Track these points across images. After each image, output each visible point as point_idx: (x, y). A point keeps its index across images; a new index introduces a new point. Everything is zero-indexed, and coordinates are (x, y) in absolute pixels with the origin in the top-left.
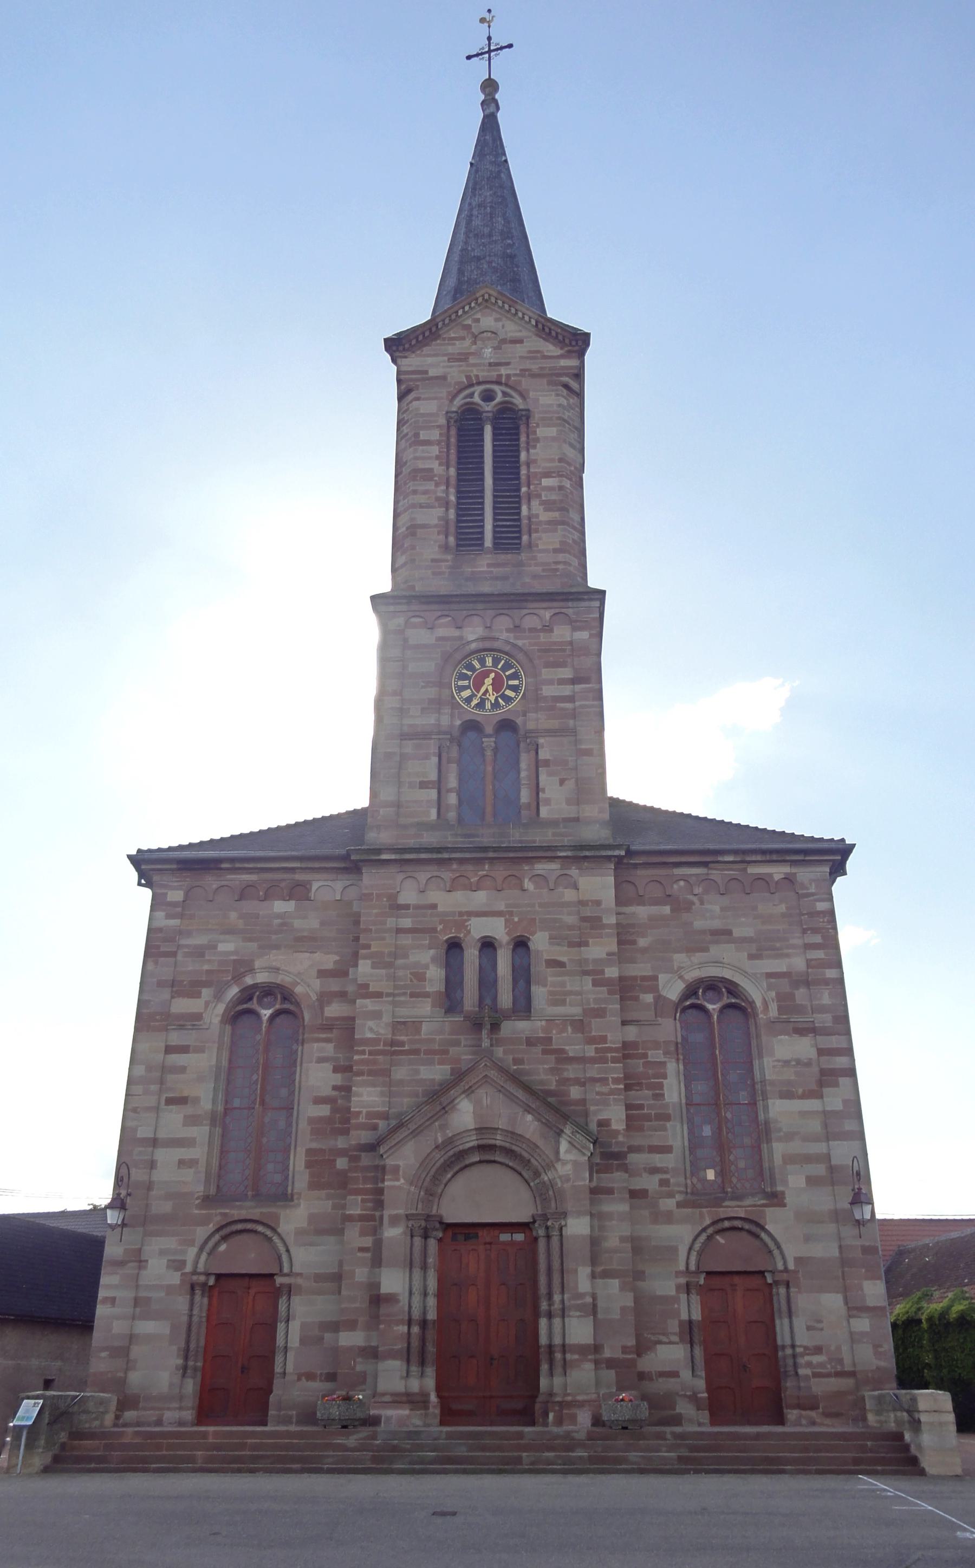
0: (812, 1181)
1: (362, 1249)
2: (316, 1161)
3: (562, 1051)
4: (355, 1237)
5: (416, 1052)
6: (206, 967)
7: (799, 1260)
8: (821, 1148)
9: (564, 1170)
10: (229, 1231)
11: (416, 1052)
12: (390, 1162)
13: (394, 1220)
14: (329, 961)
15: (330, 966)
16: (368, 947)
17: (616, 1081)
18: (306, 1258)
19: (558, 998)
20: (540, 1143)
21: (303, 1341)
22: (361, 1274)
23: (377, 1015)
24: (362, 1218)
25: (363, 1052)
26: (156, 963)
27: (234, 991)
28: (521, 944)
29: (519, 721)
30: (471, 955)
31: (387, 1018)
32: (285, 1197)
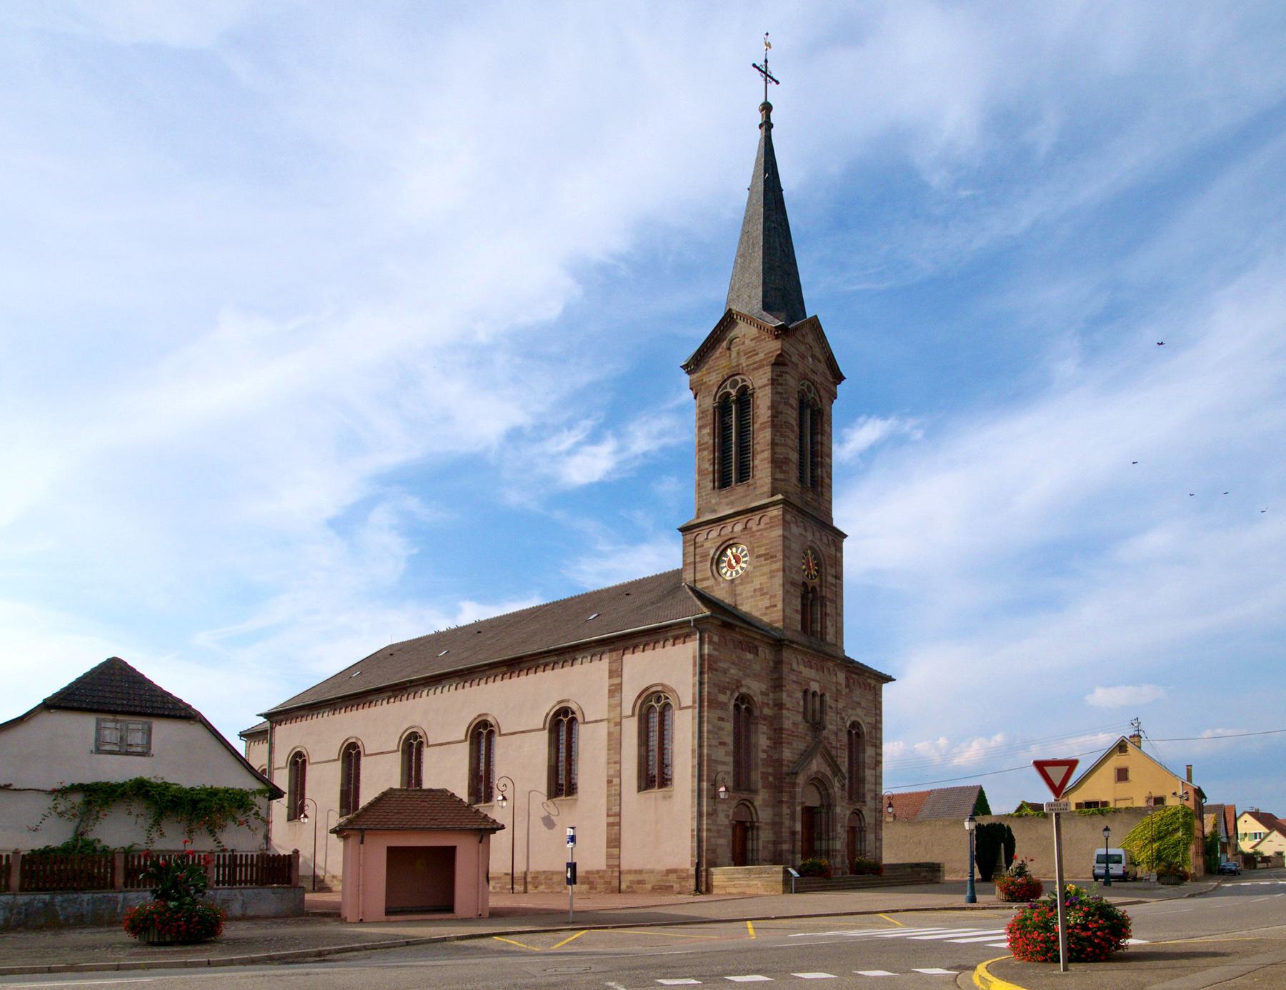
2: (765, 776)
8: (873, 787)
14: (764, 687)
18: (764, 815)
19: (832, 722)
23: (788, 718)
27: (736, 695)
28: (822, 695)
30: (810, 697)
32: (756, 792)
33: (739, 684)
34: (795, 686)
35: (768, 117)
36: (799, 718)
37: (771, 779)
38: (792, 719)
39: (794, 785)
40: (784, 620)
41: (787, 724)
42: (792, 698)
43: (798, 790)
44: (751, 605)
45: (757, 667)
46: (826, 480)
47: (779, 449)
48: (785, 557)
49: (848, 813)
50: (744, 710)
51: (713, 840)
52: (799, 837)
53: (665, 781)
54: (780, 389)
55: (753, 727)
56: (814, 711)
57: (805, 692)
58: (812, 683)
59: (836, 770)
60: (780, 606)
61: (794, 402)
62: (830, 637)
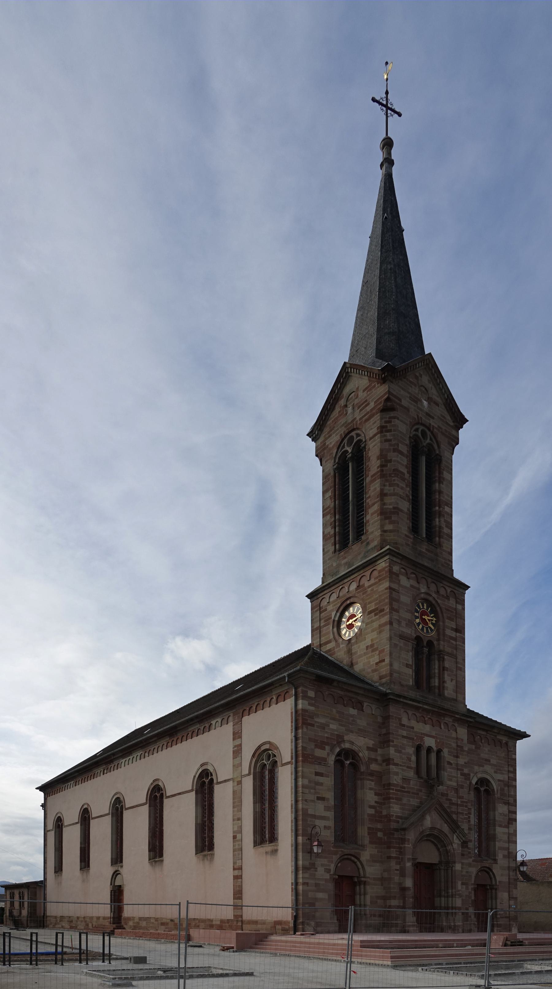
0: (504, 856)
1: (397, 870)
2: (372, 832)
3: (450, 800)
4: (393, 865)
5: (408, 792)
6: (326, 735)
7: (500, 882)
8: (506, 845)
9: (455, 846)
10: (344, 858)
11: (408, 792)
12: (407, 837)
13: (409, 860)
14: (371, 743)
15: (371, 746)
16: (393, 742)
17: (466, 814)
18: (372, 871)
19: (450, 778)
20: (449, 835)
21: (371, 902)
22: (397, 879)
23: (397, 774)
24: (396, 858)
25: (393, 789)
26: (307, 728)
27: (338, 750)
28: (439, 752)
29: (435, 642)
30: (424, 753)
31: (400, 776)
33: (340, 739)
34: (405, 741)
35: (389, 154)
36: (411, 774)
37: (380, 834)
38: (401, 773)
39: (403, 841)
40: (391, 675)
41: (396, 780)
42: (402, 754)
43: (409, 846)
44: (366, 664)
45: (362, 723)
46: (446, 530)
47: (387, 500)
48: (392, 609)
49: (473, 871)
50: (348, 764)
51: (310, 895)
52: (411, 893)
53: (273, 839)
54: (388, 435)
55: (359, 782)
56: (428, 767)
57: (418, 749)
58: (426, 739)
59: (455, 826)
60: (387, 660)
61: (404, 449)
62: (449, 692)
